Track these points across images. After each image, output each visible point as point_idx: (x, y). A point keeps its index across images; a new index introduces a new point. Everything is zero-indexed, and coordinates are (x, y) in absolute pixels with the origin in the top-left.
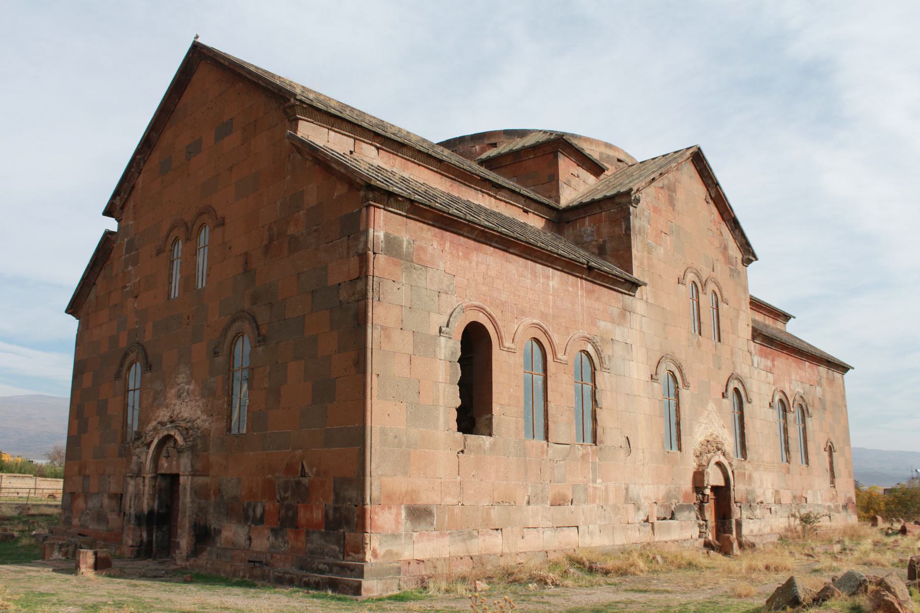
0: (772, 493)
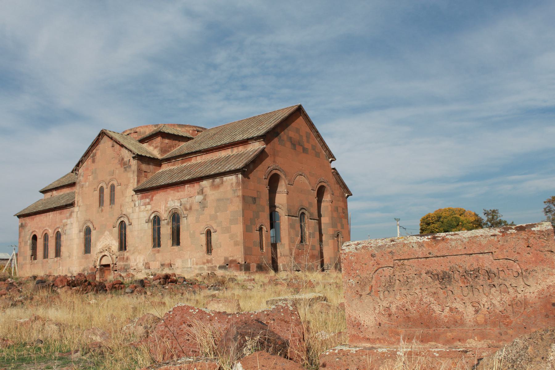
0: (143, 264)
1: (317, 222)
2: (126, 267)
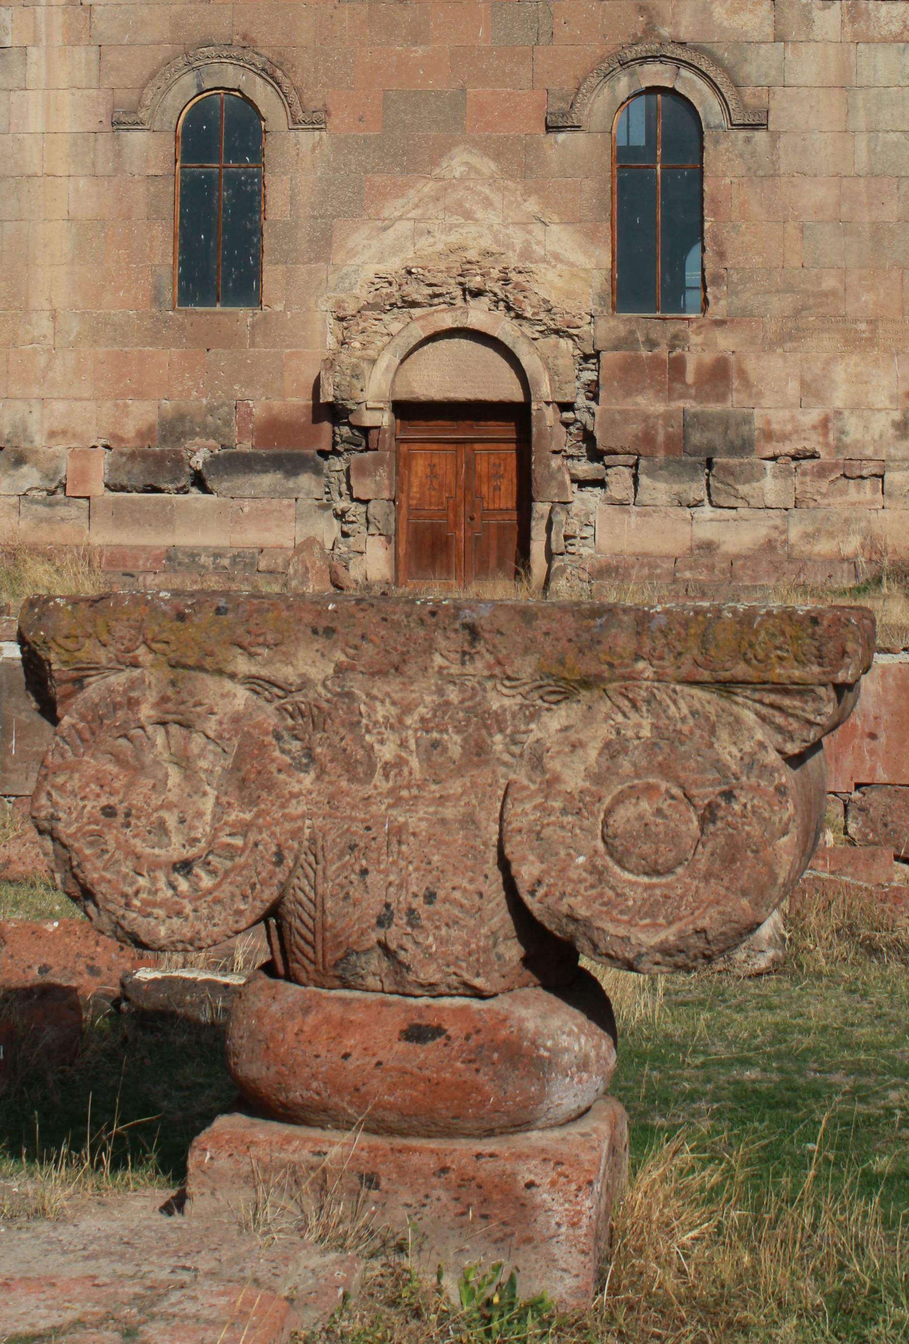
2: (697, 438)
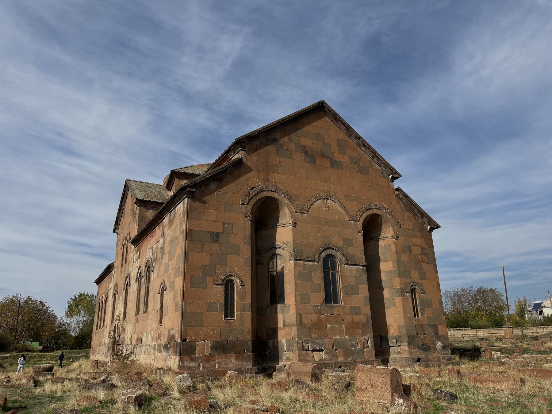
1: (363, 270)
